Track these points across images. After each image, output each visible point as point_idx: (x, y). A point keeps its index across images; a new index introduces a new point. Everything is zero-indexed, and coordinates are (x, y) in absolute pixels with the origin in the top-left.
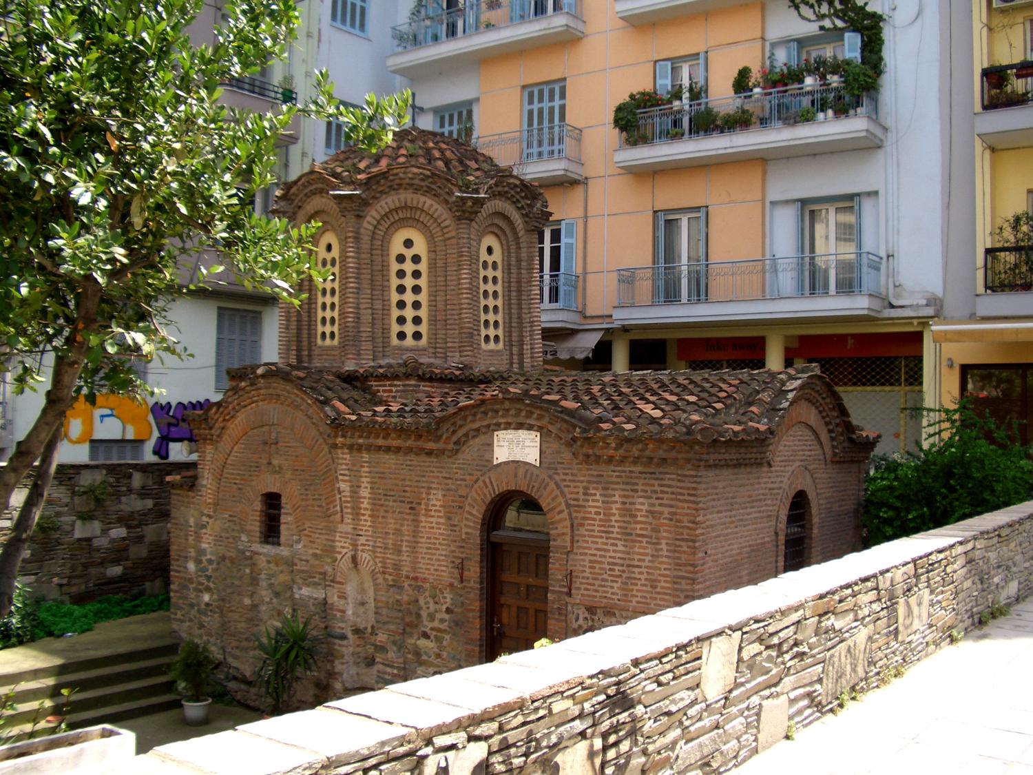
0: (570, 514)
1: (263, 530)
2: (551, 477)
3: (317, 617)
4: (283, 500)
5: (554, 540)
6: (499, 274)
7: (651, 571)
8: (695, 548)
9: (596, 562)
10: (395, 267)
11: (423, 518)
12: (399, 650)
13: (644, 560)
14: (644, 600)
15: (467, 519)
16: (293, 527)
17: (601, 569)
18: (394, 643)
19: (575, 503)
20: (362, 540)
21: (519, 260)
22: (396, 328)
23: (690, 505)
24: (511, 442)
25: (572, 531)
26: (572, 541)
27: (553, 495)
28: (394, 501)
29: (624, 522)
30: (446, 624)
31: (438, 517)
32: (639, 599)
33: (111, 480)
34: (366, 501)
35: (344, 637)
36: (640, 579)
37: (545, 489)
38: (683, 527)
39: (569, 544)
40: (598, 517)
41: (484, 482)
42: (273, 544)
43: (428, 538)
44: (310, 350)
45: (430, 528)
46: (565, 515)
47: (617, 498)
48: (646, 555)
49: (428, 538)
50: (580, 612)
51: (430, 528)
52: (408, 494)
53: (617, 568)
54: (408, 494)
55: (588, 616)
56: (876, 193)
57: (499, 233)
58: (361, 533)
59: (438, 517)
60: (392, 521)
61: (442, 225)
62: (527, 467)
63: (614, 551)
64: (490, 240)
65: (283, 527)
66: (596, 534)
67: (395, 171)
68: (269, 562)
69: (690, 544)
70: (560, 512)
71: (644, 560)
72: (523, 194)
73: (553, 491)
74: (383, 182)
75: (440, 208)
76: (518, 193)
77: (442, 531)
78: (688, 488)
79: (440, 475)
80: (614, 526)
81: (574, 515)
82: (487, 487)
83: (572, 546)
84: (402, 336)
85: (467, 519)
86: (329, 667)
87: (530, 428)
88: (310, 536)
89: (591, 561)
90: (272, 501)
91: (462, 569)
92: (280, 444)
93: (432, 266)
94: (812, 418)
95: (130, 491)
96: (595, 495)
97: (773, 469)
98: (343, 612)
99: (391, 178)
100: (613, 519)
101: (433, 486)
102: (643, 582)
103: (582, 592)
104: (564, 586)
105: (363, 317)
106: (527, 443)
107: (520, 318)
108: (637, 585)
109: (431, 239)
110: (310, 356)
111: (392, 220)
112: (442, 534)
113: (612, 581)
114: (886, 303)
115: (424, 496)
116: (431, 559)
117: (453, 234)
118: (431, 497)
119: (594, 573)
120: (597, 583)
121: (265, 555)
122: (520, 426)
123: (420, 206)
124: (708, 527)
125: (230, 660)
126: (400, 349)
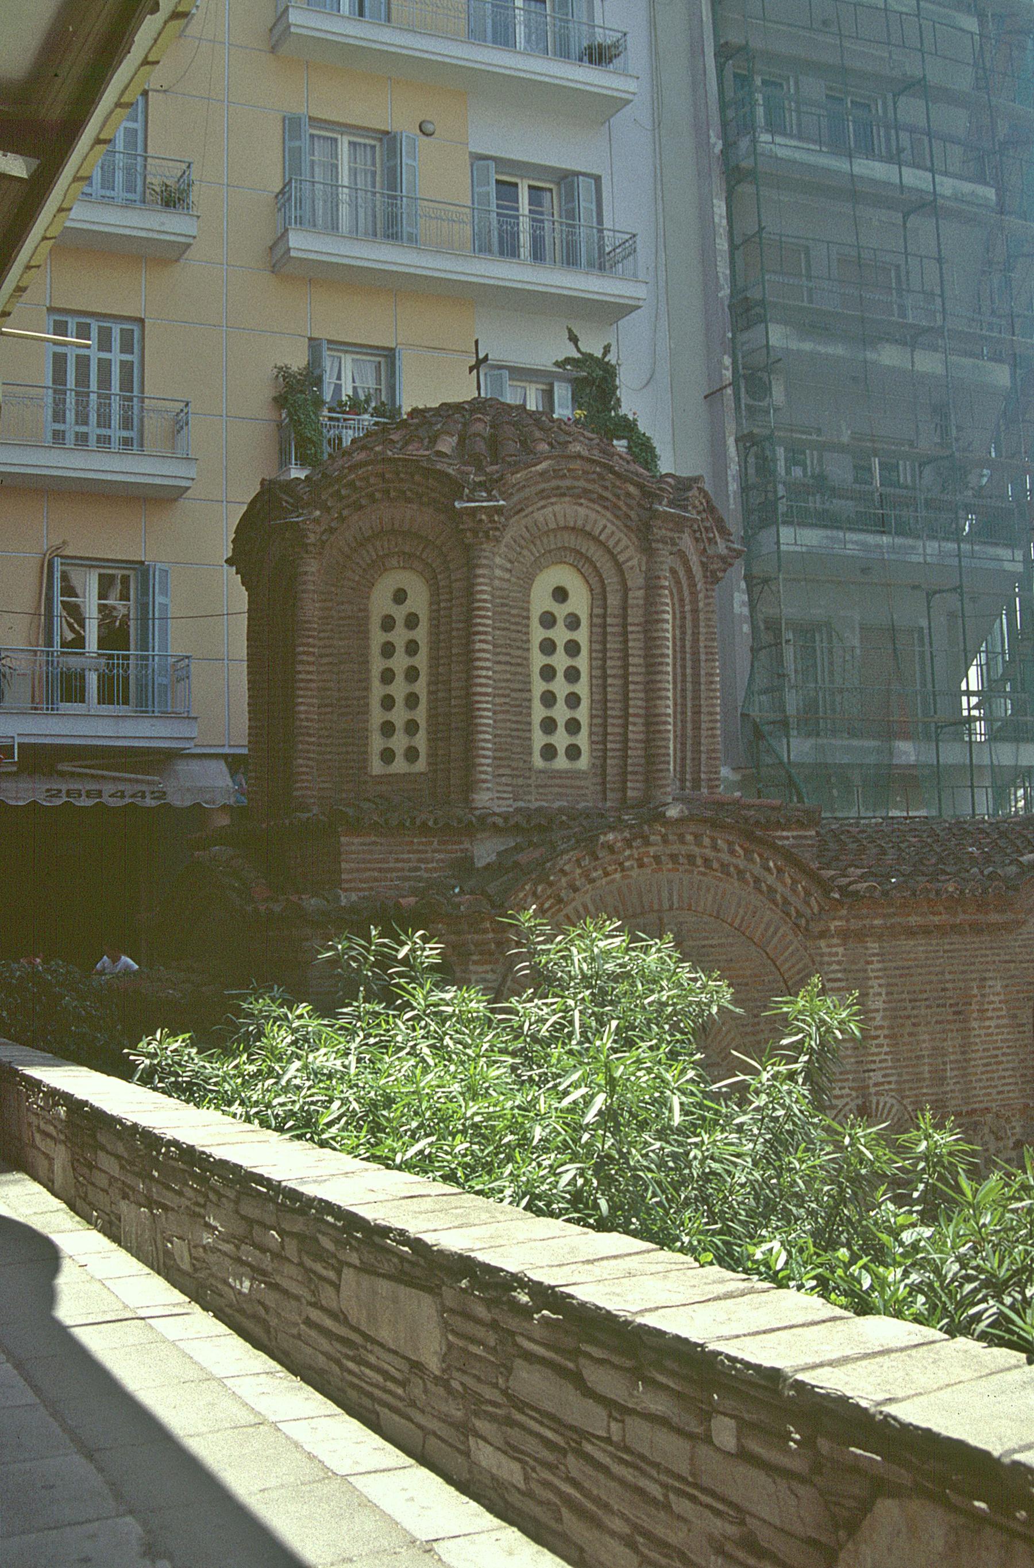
11: (975, 1024)
20: (877, 1077)
28: (928, 1007)
31: (998, 1017)
34: (878, 1016)
45: (987, 1035)
51: (987, 1035)
52: (949, 994)
54: (949, 994)
58: (873, 1066)
59: (998, 1017)
60: (926, 1037)
77: (1005, 1036)
79: (997, 958)
101: (988, 975)
112: (1007, 1040)
115: (975, 991)
116: (992, 1079)
118: (987, 990)
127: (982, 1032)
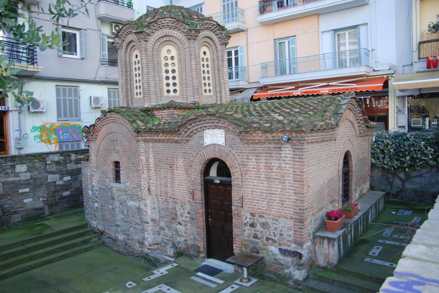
0: (240, 168)
1: (115, 177)
2: (230, 151)
3: (136, 214)
4: (121, 164)
5: (234, 181)
6: (209, 63)
7: (281, 196)
8: (303, 185)
9: (254, 191)
10: (163, 62)
11: (175, 171)
12: (169, 230)
13: (277, 191)
14: (278, 211)
15: (194, 172)
16: (125, 176)
17: (256, 195)
18: (167, 226)
19: (243, 163)
20: (151, 181)
21: (218, 57)
22: (166, 88)
23: (300, 163)
24: (212, 135)
25: (242, 177)
26: (242, 182)
27: (232, 160)
28: (163, 164)
29: (267, 172)
30: (188, 218)
31: (182, 171)
32: (276, 210)
33: (62, 158)
34: (152, 164)
35: (147, 223)
36: (276, 200)
37: (228, 157)
38: (297, 175)
39: (240, 183)
40: (254, 170)
41: (201, 154)
42: (118, 183)
43: (178, 180)
44: (132, 100)
45: (179, 175)
46: (238, 169)
47: (263, 161)
48: (279, 188)
49: (178, 180)
50: (247, 215)
51: (179, 175)
52: (169, 161)
53: (264, 195)
54: (169, 161)
55: (252, 217)
56: (367, 24)
57: (209, 45)
58: (151, 178)
59: (182, 171)
60: (163, 173)
61: (183, 42)
62: (219, 147)
63: (263, 186)
64: (204, 49)
65: (121, 176)
66: (253, 178)
67: (160, 20)
68: (117, 190)
69: (301, 183)
70: (236, 168)
71: (277, 191)
72: (218, 29)
73: (232, 158)
74: (155, 25)
75: (181, 35)
76: (215, 28)
77: (184, 177)
78: (299, 155)
79: (182, 152)
80: (262, 174)
81: (242, 169)
82: (202, 157)
83: (242, 184)
84: (168, 91)
85: (194, 172)
86: (143, 235)
87: (220, 128)
88: (131, 180)
89: (251, 191)
90: (117, 164)
91: (193, 194)
92: (118, 141)
93: (180, 61)
94: (351, 118)
95: (71, 161)
96: (252, 159)
97: (336, 142)
98: (147, 212)
99: (159, 23)
100: (261, 171)
101: (179, 157)
102: (277, 201)
103: (248, 206)
104: (239, 203)
105: (151, 84)
106: (219, 136)
107: (219, 81)
108: (274, 203)
109: (178, 49)
110: (132, 103)
111: (161, 42)
112: (184, 178)
113: (262, 201)
114: (372, 70)
115: (175, 161)
116: (180, 190)
117: (187, 46)
118: (178, 161)
119: (253, 197)
120: (255, 201)
121: (116, 188)
122: (216, 127)
123: (172, 35)
124: (309, 173)
125: (107, 230)
126: (168, 97)
127: (178, 174)
